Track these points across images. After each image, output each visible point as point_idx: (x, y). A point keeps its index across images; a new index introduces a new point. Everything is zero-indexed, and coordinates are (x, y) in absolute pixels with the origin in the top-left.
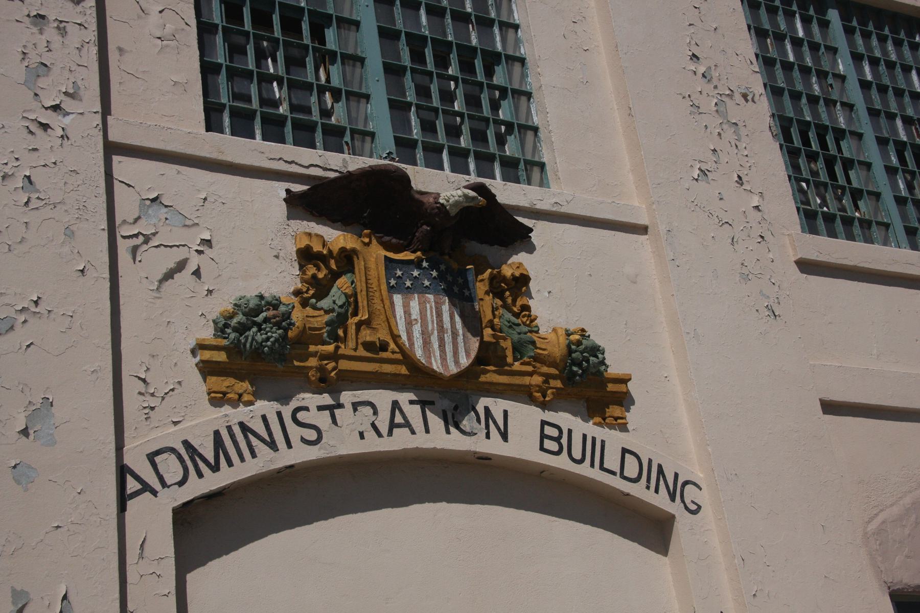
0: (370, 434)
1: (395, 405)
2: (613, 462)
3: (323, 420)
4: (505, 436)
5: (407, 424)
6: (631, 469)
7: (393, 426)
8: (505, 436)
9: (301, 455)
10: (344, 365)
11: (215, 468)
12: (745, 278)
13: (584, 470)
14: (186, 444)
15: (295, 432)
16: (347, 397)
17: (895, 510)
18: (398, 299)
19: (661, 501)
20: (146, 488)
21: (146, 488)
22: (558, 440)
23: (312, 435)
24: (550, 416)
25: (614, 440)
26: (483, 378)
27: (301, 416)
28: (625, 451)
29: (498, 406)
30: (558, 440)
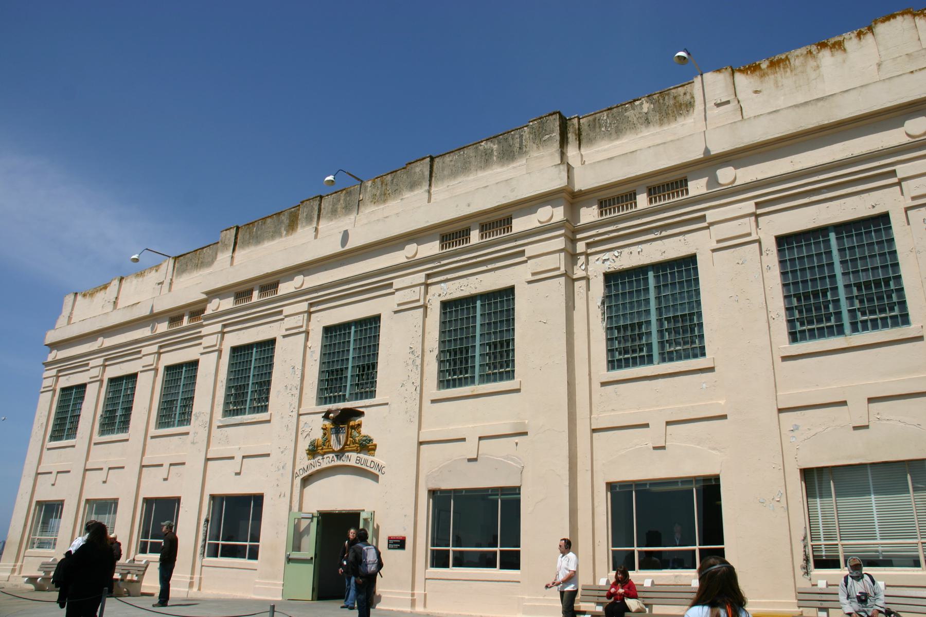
0: (328, 463)
1: (333, 457)
2: (368, 465)
3: (321, 461)
4: (350, 461)
5: (334, 460)
6: (372, 466)
7: (332, 461)
8: (350, 461)
9: (318, 468)
10: (324, 450)
11: (306, 472)
12: (406, 412)
13: (363, 467)
14: (304, 468)
15: (317, 464)
16: (325, 456)
17: (436, 469)
18: (332, 435)
19: (377, 472)
20: (298, 476)
21: (298, 476)
22: (359, 460)
23: (319, 464)
24: (359, 455)
25: (370, 458)
26: (345, 449)
27: (319, 461)
28: (372, 461)
29: (349, 454)
30: (359, 460)
